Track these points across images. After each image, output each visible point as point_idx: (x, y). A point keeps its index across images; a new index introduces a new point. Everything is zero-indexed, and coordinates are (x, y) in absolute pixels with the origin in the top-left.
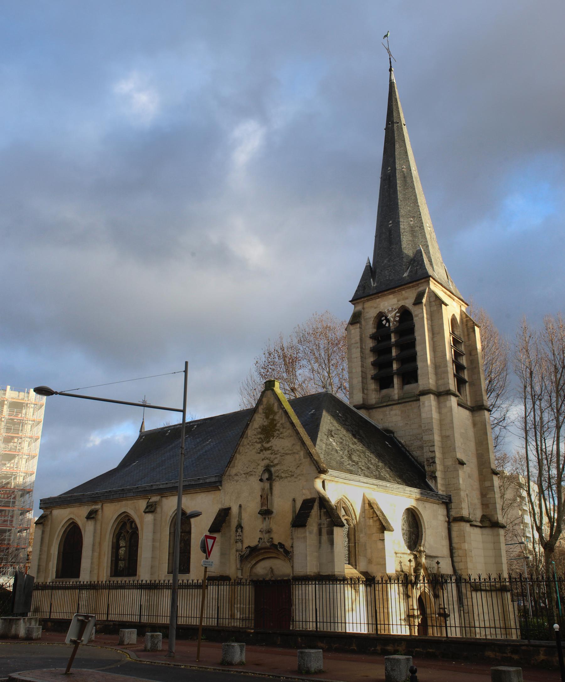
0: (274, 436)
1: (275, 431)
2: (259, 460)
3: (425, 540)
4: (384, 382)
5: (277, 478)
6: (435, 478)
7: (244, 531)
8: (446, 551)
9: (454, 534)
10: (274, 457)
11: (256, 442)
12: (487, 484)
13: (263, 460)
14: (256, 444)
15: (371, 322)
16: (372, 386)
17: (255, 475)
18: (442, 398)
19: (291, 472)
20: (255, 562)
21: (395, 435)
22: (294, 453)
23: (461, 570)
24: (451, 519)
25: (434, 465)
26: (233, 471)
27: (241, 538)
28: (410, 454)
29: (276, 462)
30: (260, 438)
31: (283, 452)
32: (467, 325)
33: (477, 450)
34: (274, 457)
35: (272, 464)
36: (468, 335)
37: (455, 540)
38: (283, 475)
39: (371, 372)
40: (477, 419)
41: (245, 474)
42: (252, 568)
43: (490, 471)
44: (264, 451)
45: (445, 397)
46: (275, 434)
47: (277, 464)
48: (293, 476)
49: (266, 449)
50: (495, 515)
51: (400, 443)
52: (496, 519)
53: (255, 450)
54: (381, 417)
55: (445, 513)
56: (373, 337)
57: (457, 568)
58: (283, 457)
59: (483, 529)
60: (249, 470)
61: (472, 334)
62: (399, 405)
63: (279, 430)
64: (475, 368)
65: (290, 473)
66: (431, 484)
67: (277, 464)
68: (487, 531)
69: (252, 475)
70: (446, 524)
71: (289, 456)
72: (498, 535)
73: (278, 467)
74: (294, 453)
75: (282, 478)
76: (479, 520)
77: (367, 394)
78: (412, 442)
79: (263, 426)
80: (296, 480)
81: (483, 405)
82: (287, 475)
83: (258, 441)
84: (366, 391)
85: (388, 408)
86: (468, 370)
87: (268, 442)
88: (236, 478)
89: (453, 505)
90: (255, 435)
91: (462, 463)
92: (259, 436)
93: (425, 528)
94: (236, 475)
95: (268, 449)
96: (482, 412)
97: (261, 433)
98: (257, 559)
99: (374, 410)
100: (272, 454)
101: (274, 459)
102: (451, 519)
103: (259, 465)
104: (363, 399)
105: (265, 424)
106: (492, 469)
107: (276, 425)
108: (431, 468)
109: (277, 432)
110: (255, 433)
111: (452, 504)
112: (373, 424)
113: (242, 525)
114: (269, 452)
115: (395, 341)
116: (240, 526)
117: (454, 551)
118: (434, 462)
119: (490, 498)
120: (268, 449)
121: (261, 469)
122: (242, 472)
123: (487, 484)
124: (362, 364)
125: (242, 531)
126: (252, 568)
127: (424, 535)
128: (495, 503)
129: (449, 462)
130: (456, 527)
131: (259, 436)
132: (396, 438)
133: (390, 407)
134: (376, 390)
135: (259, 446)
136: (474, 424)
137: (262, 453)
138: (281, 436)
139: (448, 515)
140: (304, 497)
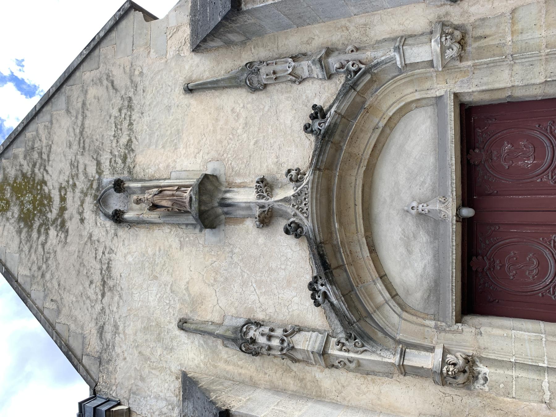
0: (44, 182)
1: (34, 180)
2: (81, 236)
5: (129, 160)
7: (260, 316)
10: (82, 177)
11: (43, 245)
13: (82, 220)
14: (47, 246)
17: (111, 251)
19: (120, 110)
20: (380, 285)
22: (84, 104)
26: (94, 345)
27: (279, 332)
29: (92, 170)
30: (39, 232)
31: (75, 147)
34: (82, 177)
35: (95, 186)
38: (124, 140)
41: (103, 295)
42: (403, 307)
44: (66, 215)
46: (39, 176)
47: (99, 164)
48: (130, 99)
49: (63, 209)
53: (58, 249)
58: (87, 146)
60: (97, 278)
63: (34, 165)
65: (124, 111)
67: (99, 164)
69: (109, 268)
71: (87, 122)
73: (105, 159)
74: (84, 104)
75: (130, 141)
79: (20, 219)
80: (140, 88)
82: (126, 124)
83: (43, 238)
87: (50, 199)
88: (108, 336)
90: (31, 247)
92: (35, 235)
94: (101, 331)
95: (63, 199)
97: (30, 227)
98: (369, 272)
100: (74, 185)
101: (86, 174)
103: (91, 236)
105: (15, 210)
107: (24, 175)
109: (36, 170)
110: (26, 248)
113: (241, 322)
114: (69, 196)
116: (243, 340)
120: (63, 199)
121: (100, 228)
122: (98, 307)
125: (258, 324)
126: (403, 307)
131: (35, 235)
135: (52, 232)
137: (68, 224)
138: (45, 157)
140: (187, 50)
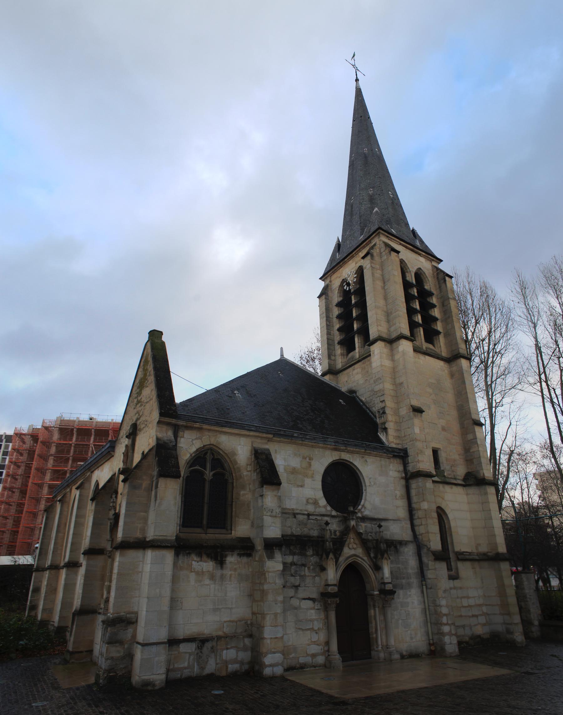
3: (365, 500)
4: (348, 345)
6: (385, 429)
8: (402, 513)
9: (413, 492)
12: (470, 437)
15: (337, 292)
16: (339, 350)
18: (395, 345)
21: (358, 394)
23: (422, 534)
24: (409, 474)
25: (385, 416)
28: (370, 411)
32: (438, 278)
33: (457, 402)
36: (440, 287)
37: (414, 499)
39: (337, 337)
40: (454, 368)
43: (471, 422)
45: (397, 343)
50: (481, 472)
51: (361, 401)
52: (482, 475)
54: (346, 379)
55: (401, 468)
56: (339, 305)
57: (417, 533)
59: (467, 488)
61: (443, 285)
62: (360, 363)
64: (449, 317)
66: (382, 437)
68: (473, 490)
70: (403, 482)
72: (486, 494)
76: (462, 478)
77: (335, 360)
78: (371, 398)
81: (459, 353)
84: (333, 358)
85: (351, 368)
86: (442, 322)
89: (410, 459)
91: (418, 411)
93: (365, 486)
96: (458, 361)
99: (340, 374)
102: (409, 474)
104: (329, 364)
106: (473, 420)
108: (382, 420)
111: (409, 458)
112: (333, 385)
115: (355, 302)
117: (414, 512)
118: (384, 413)
119: (474, 452)
123: (470, 437)
124: (327, 332)
127: (364, 494)
128: (480, 457)
129: (404, 411)
130: (414, 484)
132: (358, 397)
133: (353, 367)
134: (342, 354)
136: (452, 375)
139: (405, 470)
